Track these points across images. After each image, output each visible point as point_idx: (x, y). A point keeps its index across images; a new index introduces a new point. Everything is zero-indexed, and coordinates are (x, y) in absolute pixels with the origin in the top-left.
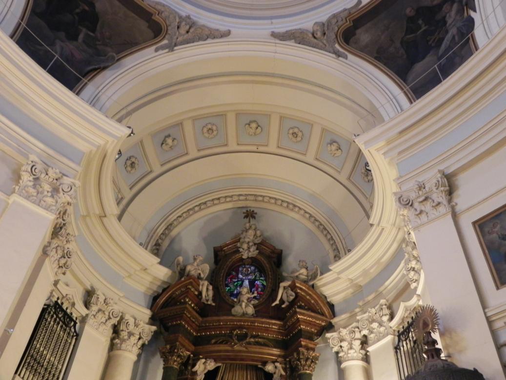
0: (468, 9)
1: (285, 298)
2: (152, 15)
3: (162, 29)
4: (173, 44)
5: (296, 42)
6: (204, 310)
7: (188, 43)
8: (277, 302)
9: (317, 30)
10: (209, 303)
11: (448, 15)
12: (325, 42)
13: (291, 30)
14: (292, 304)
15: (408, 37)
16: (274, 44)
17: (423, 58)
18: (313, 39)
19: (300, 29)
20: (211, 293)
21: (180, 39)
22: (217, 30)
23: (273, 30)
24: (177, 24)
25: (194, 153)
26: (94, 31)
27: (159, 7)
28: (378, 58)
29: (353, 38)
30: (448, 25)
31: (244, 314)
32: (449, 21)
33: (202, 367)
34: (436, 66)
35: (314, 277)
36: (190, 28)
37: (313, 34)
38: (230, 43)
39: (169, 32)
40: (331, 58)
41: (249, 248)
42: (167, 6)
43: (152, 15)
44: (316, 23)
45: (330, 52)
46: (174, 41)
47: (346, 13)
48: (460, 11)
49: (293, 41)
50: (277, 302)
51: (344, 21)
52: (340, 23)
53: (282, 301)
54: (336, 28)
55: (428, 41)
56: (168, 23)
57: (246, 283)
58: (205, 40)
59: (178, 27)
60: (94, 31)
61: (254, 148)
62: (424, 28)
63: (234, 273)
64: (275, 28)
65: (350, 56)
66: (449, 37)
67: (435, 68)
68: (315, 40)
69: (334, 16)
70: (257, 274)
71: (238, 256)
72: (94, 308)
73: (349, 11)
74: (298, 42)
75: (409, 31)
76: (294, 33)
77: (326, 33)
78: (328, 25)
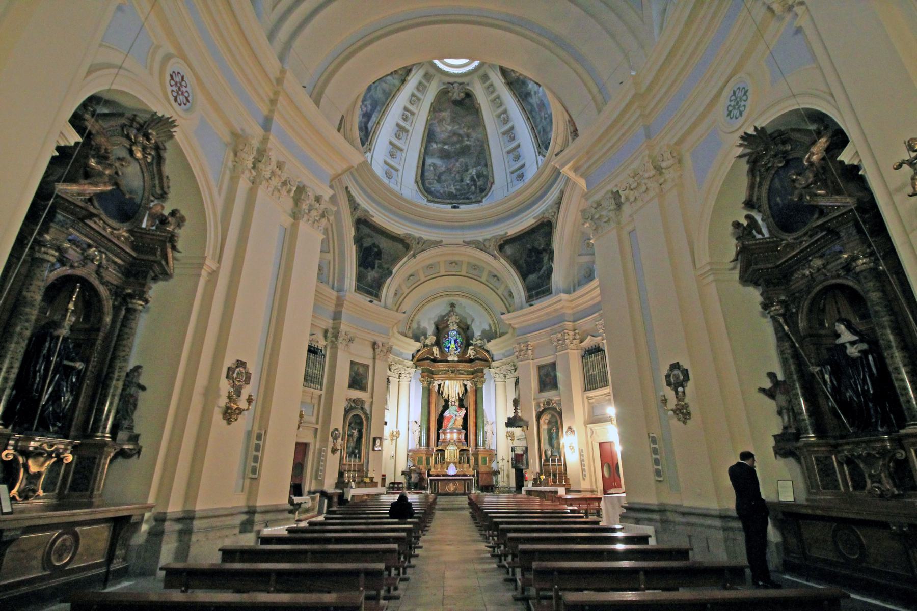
1: (471, 354)
6: (435, 360)
8: (468, 355)
10: (438, 356)
14: (474, 356)
20: (438, 352)
25: (423, 279)
31: (453, 361)
32: (545, 262)
33: (436, 384)
35: (485, 345)
41: (453, 325)
49: (474, 246)
50: (468, 355)
53: (470, 356)
57: (453, 341)
59: (418, 243)
61: (454, 273)
62: (534, 258)
63: (447, 336)
65: (502, 260)
70: (458, 336)
71: (448, 329)
72: (392, 370)
73: (502, 237)
75: (529, 256)
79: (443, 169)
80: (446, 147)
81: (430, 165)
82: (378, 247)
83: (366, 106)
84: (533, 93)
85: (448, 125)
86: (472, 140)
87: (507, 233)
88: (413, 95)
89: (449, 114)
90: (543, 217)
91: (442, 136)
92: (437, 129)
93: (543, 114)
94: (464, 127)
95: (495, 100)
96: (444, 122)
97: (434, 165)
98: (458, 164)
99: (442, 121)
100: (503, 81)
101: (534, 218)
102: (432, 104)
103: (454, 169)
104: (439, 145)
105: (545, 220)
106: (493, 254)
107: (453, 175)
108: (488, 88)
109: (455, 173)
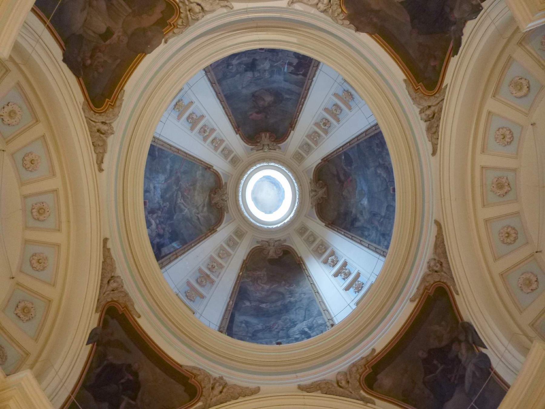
0: (478, 347)
2: (188, 379)
3: (196, 390)
4: (207, 405)
5: (322, 393)
7: (222, 403)
9: (341, 380)
11: (459, 354)
12: (350, 390)
13: (316, 382)
15: (428, 377)
16: (302, 397)
17: (451, 396)
18: (338, 388)
19: (325, 380)
21: (214, 400)
22: (248, 388)
23: (298, 383)
24: (211, 386)
26: (134, 399)
27: (195, 372)
28: (403, 401)
29: (376, 383)
30: (463, 363)
32: (463, 359)
34: (472, 403)
36: (223, 388)
37: (338, 383)
38: (261, 399)
39: (204, 394)
40: (361, 406)
42: (202, 369)
43: (188, 379)
44: (339, 373)
45: (357, 399)
46: (208, 402)
47: (364, 361)
48: (470, 348)
49: (319, 391)
51: (364, 368)
52: (361, 371)
54: (358, 376)
55: (450, 380)
56: (203, 385)
58: (237, 399)
59: (213, 388)
60: (134, 399)
62: (441, 368)
64: (301, 381)
66: (468, 373)
67: (472, 405)
68: (341, 389)
69: (354, 365)
74: (325, 392)
76: (319, 384)
77: (350, 381)
78: (350, 374)
79: (260, 327)
80: (264, 306)
81: (242, 322)
82: (136, 374)
83: (164, 230)
84: (358, 216)
85: (265, 284)
86: (297, 295)
87: (374, 350)
88: (222, 248)
89: (266, 273)
90: (426, 288)
91: (258, 294)
92: (251, 288)
93: (376, 223)
94: (285, 285)
95: (319, 247)
96: (259, 281)
97: (247, 323)
98: (280, 322)
99: (257, 281)
100: (324, 224)
101: (412, 300)
102: (244, 261)
103: (276, 327)
104: (254, 304)
105: (431, 291)
106: (358, 397)
107: (274, 333)
108: (308, 238)
109: (277, 330)
